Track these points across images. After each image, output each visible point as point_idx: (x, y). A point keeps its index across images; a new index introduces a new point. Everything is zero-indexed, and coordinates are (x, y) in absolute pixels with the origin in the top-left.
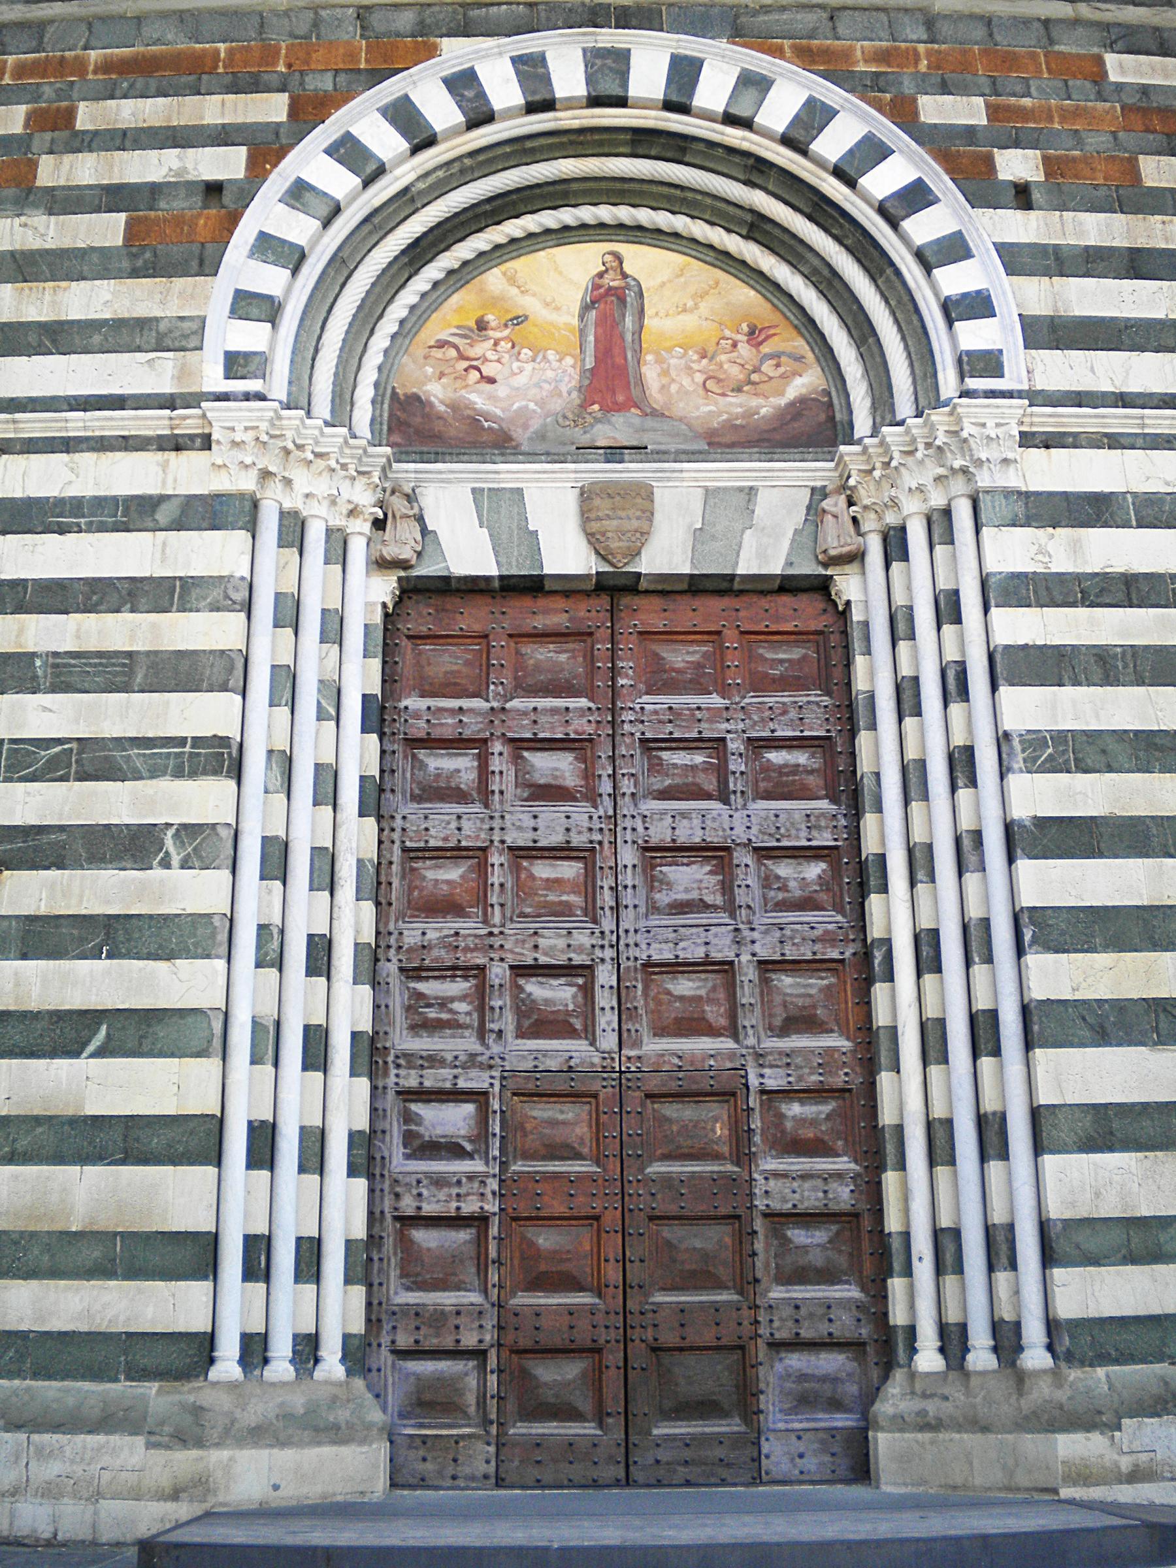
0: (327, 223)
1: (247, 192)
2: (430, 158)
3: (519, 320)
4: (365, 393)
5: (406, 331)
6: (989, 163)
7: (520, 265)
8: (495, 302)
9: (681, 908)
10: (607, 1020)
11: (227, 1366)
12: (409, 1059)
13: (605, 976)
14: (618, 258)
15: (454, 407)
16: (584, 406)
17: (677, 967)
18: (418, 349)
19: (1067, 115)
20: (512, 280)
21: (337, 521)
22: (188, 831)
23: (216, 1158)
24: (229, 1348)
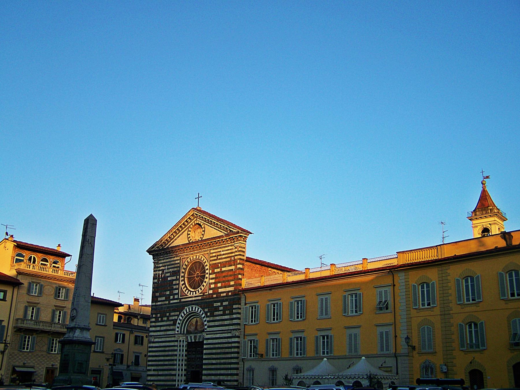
0: (181, 321)
1: (177, 320)
2: (185, 315)
3: (193, 324)
4: (185, 330)
5: (188, 325)
6: (207, 314)
7: (193, 320)
8: (192, 323)
9: (198, 361)
10: (195, 368)
11: (177, 386)
12: (188, 370)
13: (195, 365)
14: (197, 319)
15: (190, 330)
16: (195, 330)
17: (198, 365)
18: (188, 326)
19: (212, 309)
20: (192, 321)
21: (183, 339)
22: (175, 359)
23: (176, 376)
24: (177, 385)
